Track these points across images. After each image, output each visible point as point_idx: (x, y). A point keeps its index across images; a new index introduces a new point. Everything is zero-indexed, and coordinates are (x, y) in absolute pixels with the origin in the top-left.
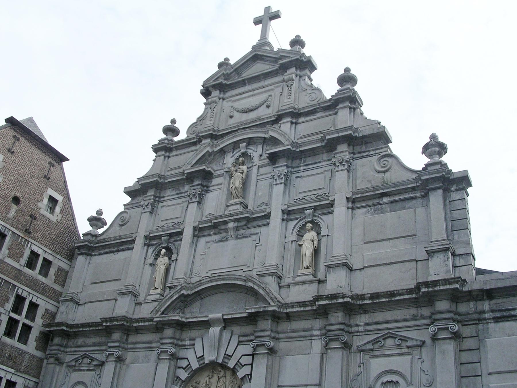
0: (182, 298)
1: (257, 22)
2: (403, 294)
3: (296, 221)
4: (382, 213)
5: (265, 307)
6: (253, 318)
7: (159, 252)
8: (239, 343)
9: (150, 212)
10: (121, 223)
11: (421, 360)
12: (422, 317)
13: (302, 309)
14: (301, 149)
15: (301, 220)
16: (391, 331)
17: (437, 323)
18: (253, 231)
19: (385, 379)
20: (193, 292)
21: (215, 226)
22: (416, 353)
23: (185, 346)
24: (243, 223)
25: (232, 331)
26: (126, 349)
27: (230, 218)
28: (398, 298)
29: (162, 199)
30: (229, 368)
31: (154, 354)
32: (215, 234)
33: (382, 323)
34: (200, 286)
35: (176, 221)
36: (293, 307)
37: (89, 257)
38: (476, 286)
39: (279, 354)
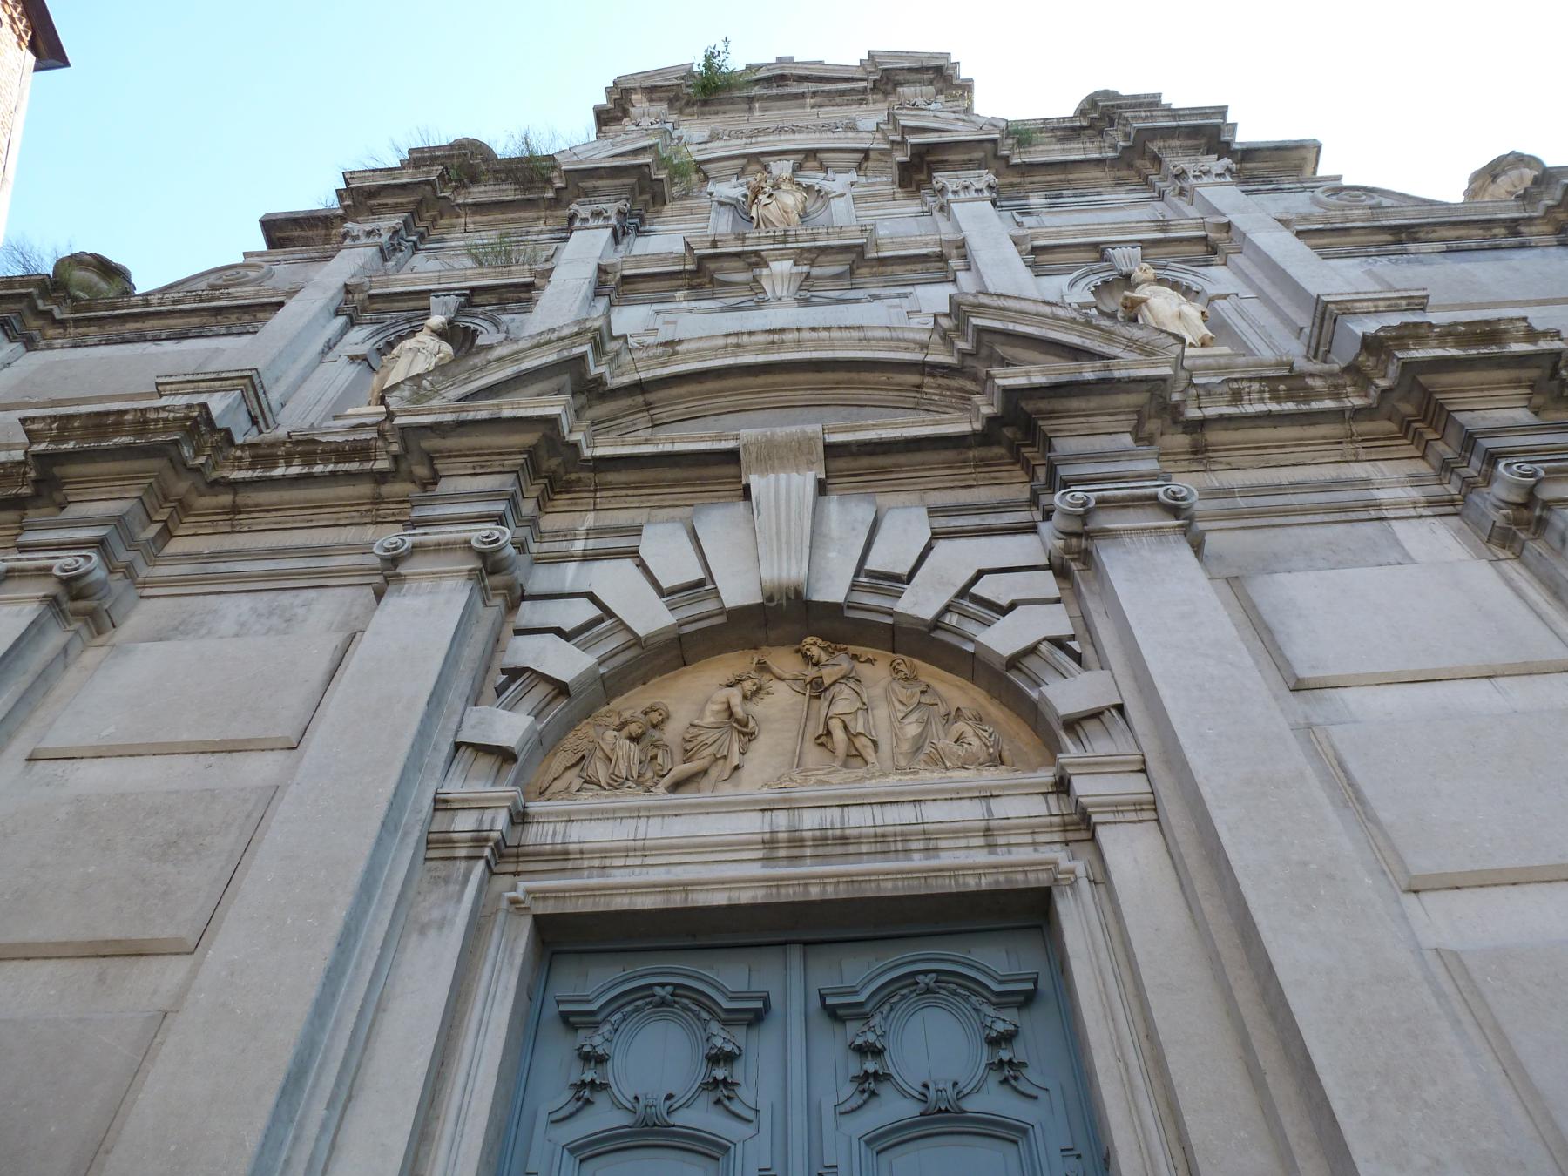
9: (382, 250)
34: (664, 364)
37: (18, 347)
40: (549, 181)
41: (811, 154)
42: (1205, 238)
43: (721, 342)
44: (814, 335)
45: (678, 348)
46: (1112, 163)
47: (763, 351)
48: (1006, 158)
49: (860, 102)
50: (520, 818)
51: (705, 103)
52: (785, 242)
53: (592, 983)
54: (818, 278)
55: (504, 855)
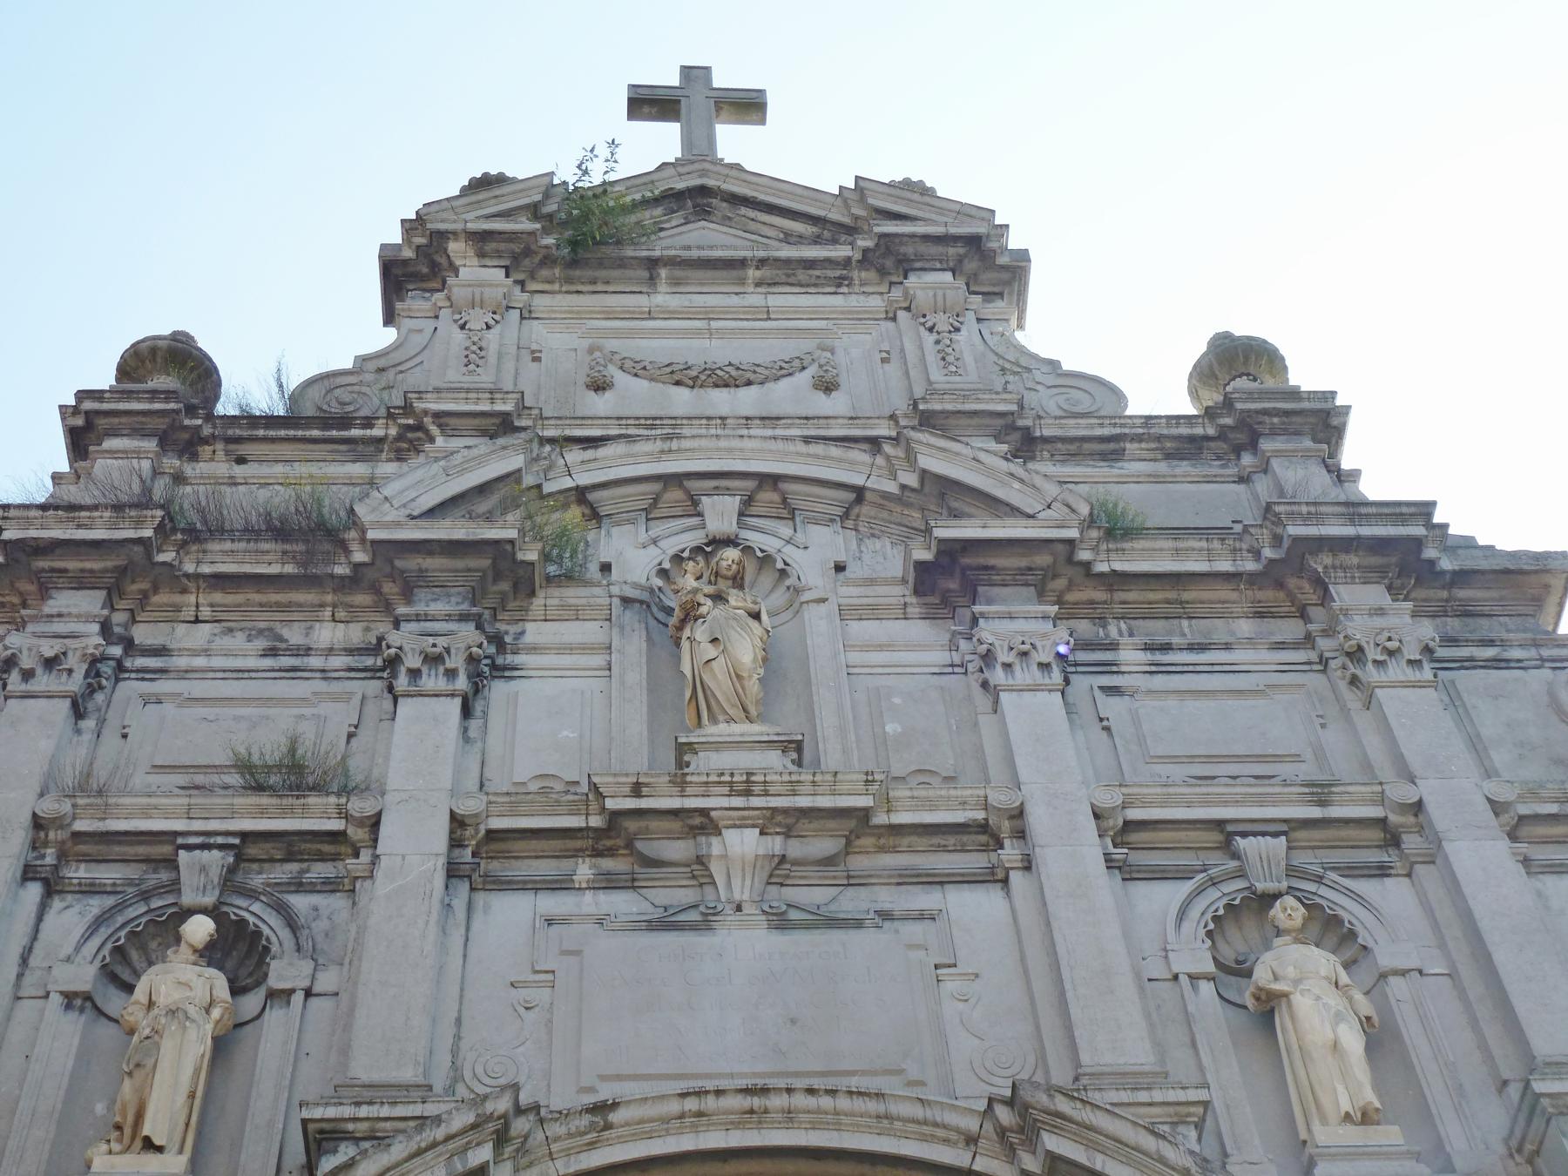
1: (648, 104)
3: (1187, 887)
7: (168, 927)
14: (1118, 566)
15: (1214, 882)
27: (738, 802)
29: (141, 662)
32: (608, 883)
34: (592, 1145)
40: (344, 546)
41: (773, 480)
42: (1382, 822)
43: (674, 1107)
44: (811, 1102)
45: (614, 1117)
46: (1252, 579)
47: (737, 1125)
48: (1087, 565)
49: (839, 282)
51: (574, 263)
52: (748, 793)
54: (796, 863)
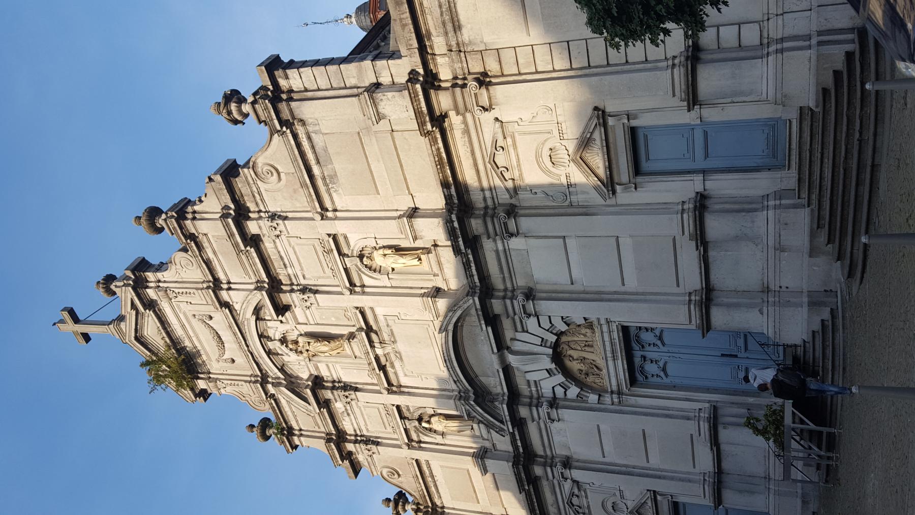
0: (480, 400)
2: (438, 149)
3: (363, 276)
4: (336, 175)
5: (476, 310)
6: (492, 320)
8: (525, 331)
10: (396, 476)
11: (519, 121)
12: (465, 122)
13: (473, 265)
16: (487, 160)
17: (469, 106)
18: (382, 323)
19: (549, 164)
20: (470, 388)
21: (382, 368)
22: (510, 128)
23: (537, 390)
24: (373, 336)
25: (512, 339)
26: (553, 456)
28: (444, 155)
30: (557, 340)
31: (555, 426)
32: (393, 366)
33: (478, 171)
35: (383, 413)
36: (472, 276)
38: (417, 59)
39: (531, 285)
50: (612, 392)
53: (640, 378)
55: (620, 393)
